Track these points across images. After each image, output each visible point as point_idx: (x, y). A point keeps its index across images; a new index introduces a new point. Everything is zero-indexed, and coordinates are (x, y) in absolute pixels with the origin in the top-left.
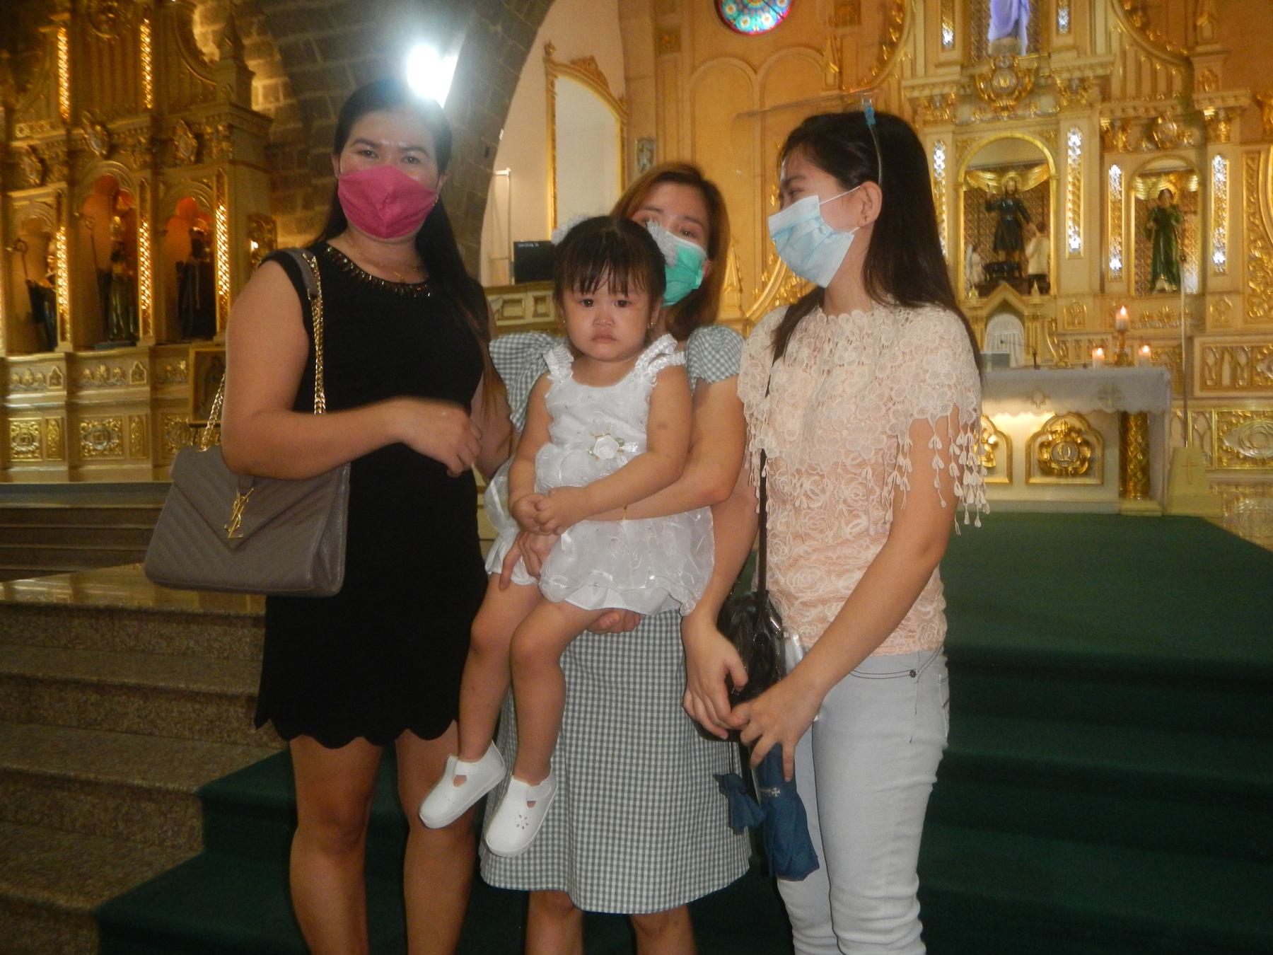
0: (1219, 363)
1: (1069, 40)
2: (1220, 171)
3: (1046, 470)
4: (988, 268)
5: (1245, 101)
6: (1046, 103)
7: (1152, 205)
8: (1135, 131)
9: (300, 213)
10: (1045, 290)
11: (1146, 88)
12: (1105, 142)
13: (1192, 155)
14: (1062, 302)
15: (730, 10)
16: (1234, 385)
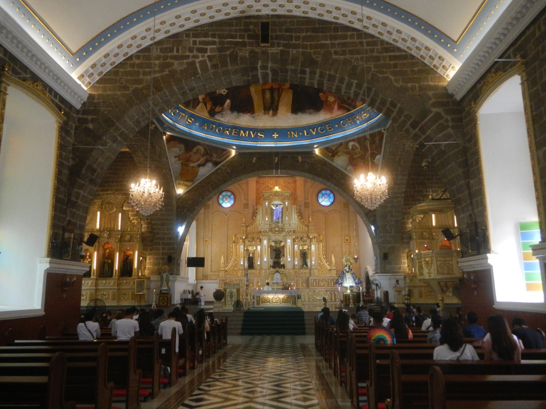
0: (314, 282)
1: (288, 223)
2: (313, 247)
3: (284, 302)
4: (274, 263)
5: (317, 235)
6: (284, 233)
7: (303, 251)
8: (299, 239)
9: (149, 252)
10: (284, 268)
11: (301, 230)
12: (294, 240)
13: (309, 244)
14: (287, 270)
15: (221, 202)
16: (316, 286)
